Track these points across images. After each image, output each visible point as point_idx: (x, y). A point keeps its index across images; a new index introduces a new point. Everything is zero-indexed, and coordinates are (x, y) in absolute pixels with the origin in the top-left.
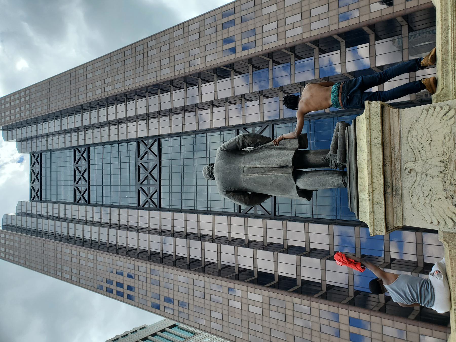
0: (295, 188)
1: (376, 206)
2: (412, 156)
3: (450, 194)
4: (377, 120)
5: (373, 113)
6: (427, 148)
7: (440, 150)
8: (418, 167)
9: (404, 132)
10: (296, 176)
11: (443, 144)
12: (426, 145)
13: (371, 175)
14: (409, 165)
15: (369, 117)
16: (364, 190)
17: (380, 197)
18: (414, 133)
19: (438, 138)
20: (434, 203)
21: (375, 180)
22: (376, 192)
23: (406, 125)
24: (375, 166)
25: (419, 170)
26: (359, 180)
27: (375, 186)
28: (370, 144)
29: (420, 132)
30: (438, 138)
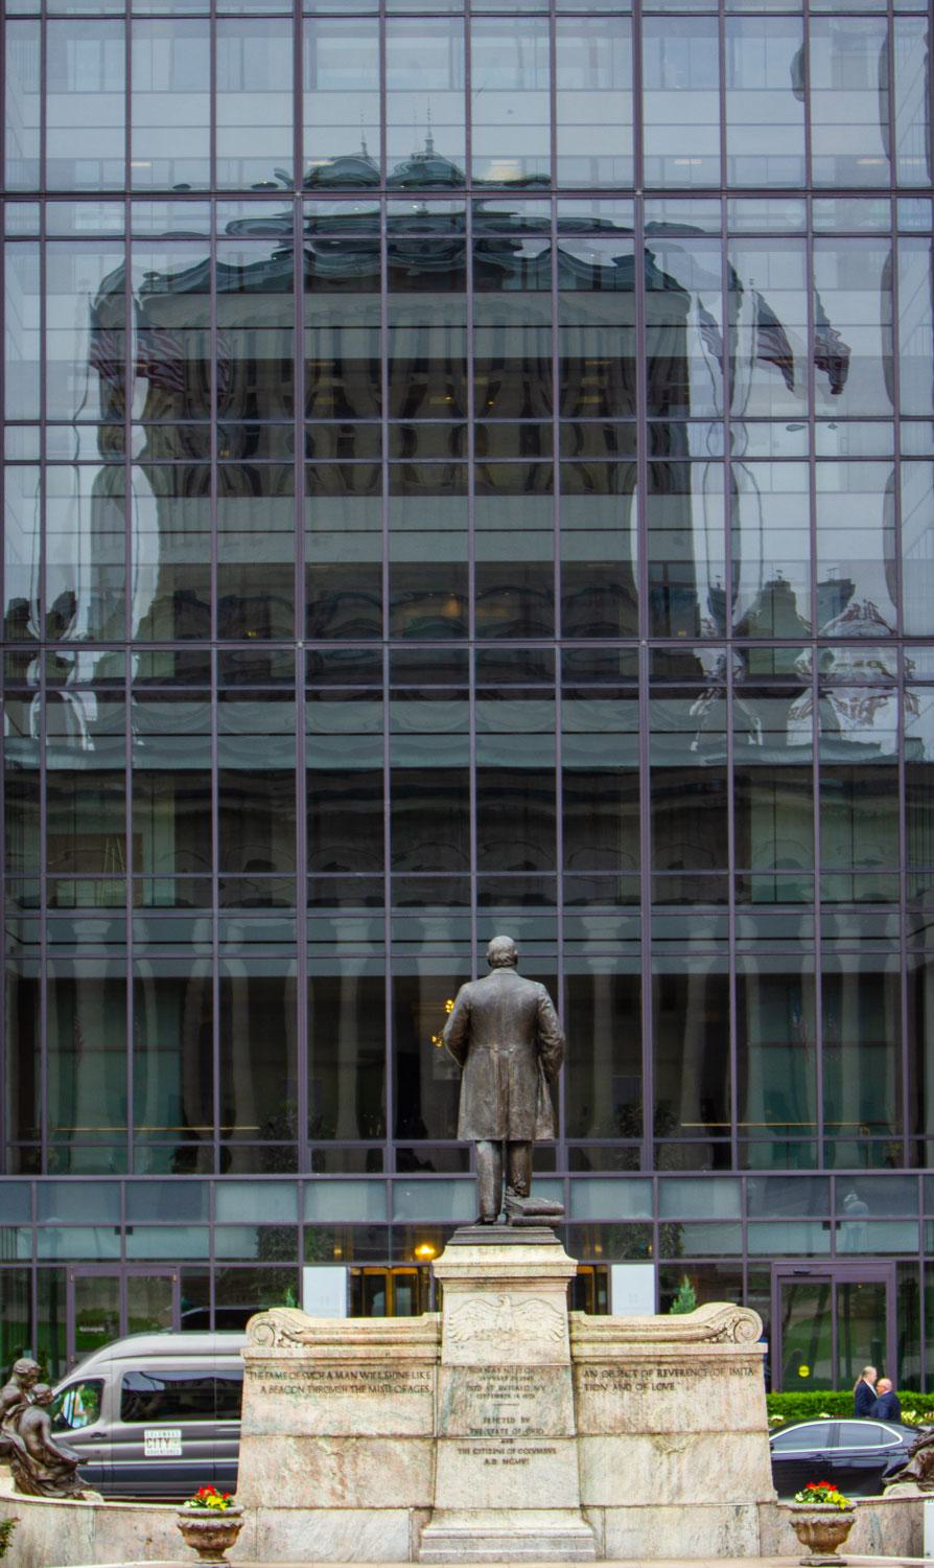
0: (478, 1138)
1: (465, 1270)
2: (517, 1302)
3: (480, 1335)
4: (556, 1272)
5: (564, 1269)
6: (524, 1317)
7: (521, 1328)
8: (506, 1308)
9: (540, 1296)
10: (497, 1144)
11: (527, 1331)
12: (527, 1316)
13: (497, 1266)
14: (507, 1301)
15: (559, 1265)
16: (481, 1253)
17: (474, 1273)
18: (540, 1305)
19: (533, 1327)
20: (470, 1321)
21: (493, 1269)
22: (479, 1269)
23: (548, 1297)
24: (507, 1269)
25: (503, 1309)
26: (492, 1247)
27: (486, 1269)
28: (531, 1265)
29: (541, 1311)
30: (533, 1327)
